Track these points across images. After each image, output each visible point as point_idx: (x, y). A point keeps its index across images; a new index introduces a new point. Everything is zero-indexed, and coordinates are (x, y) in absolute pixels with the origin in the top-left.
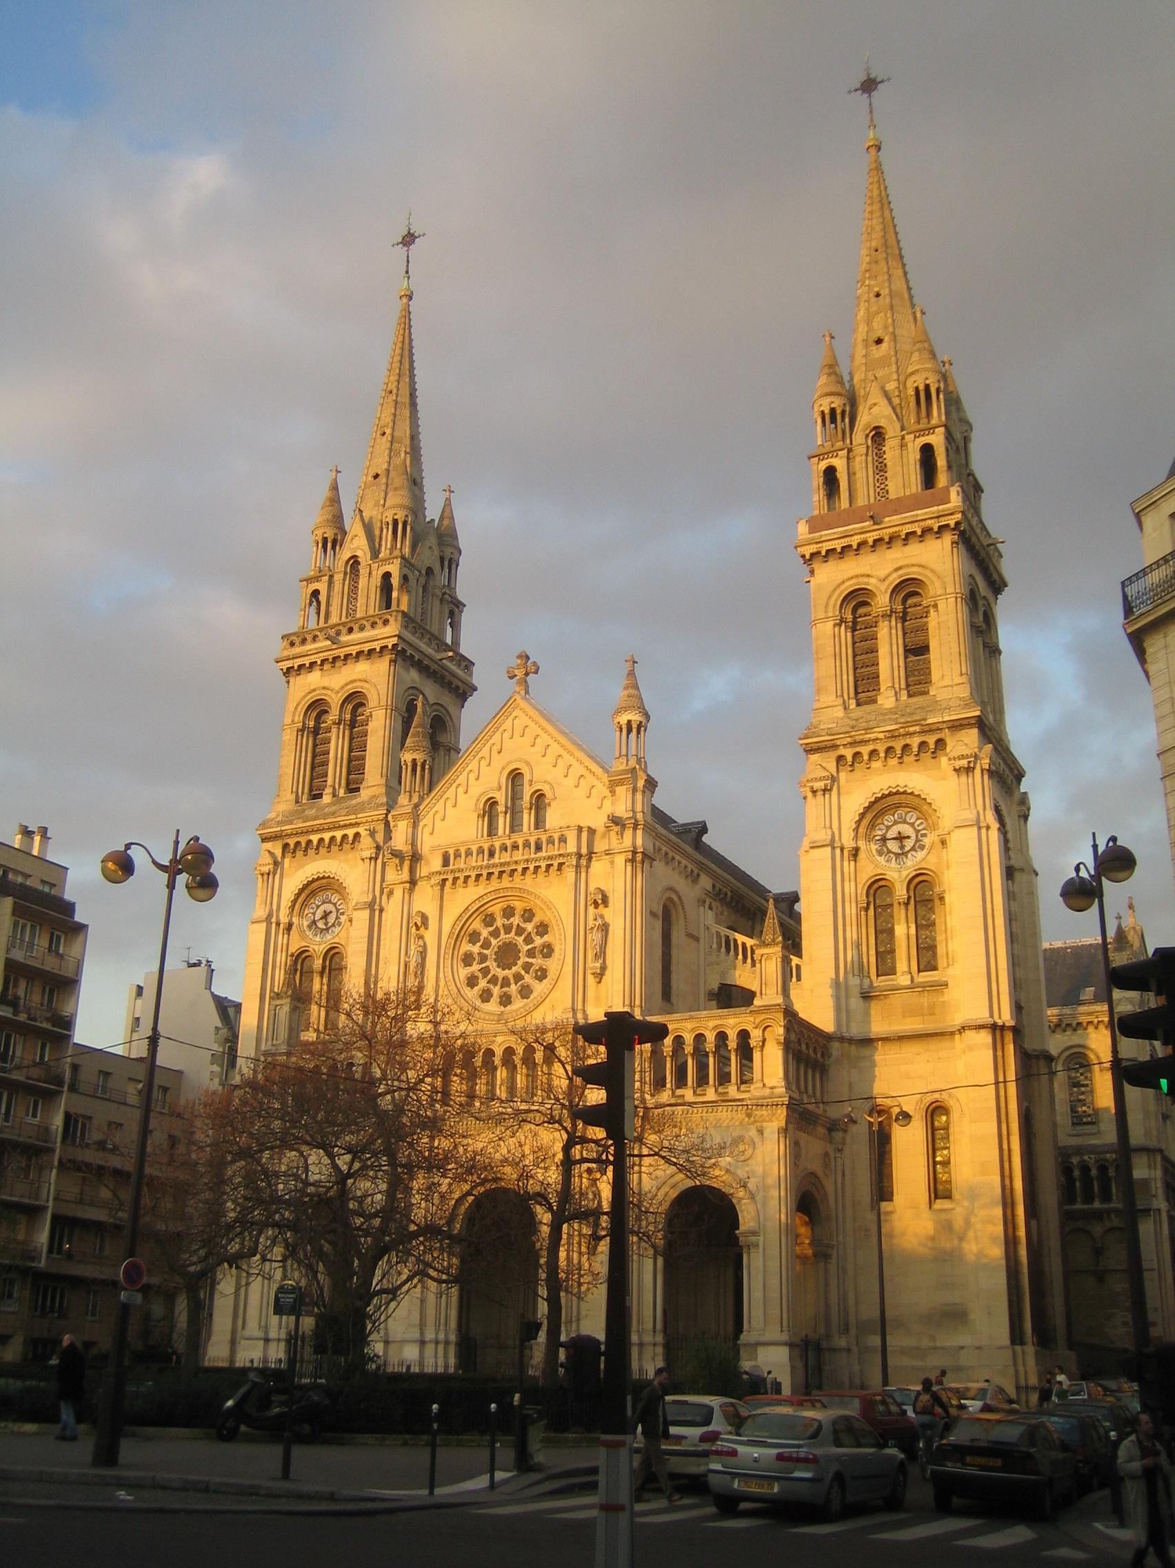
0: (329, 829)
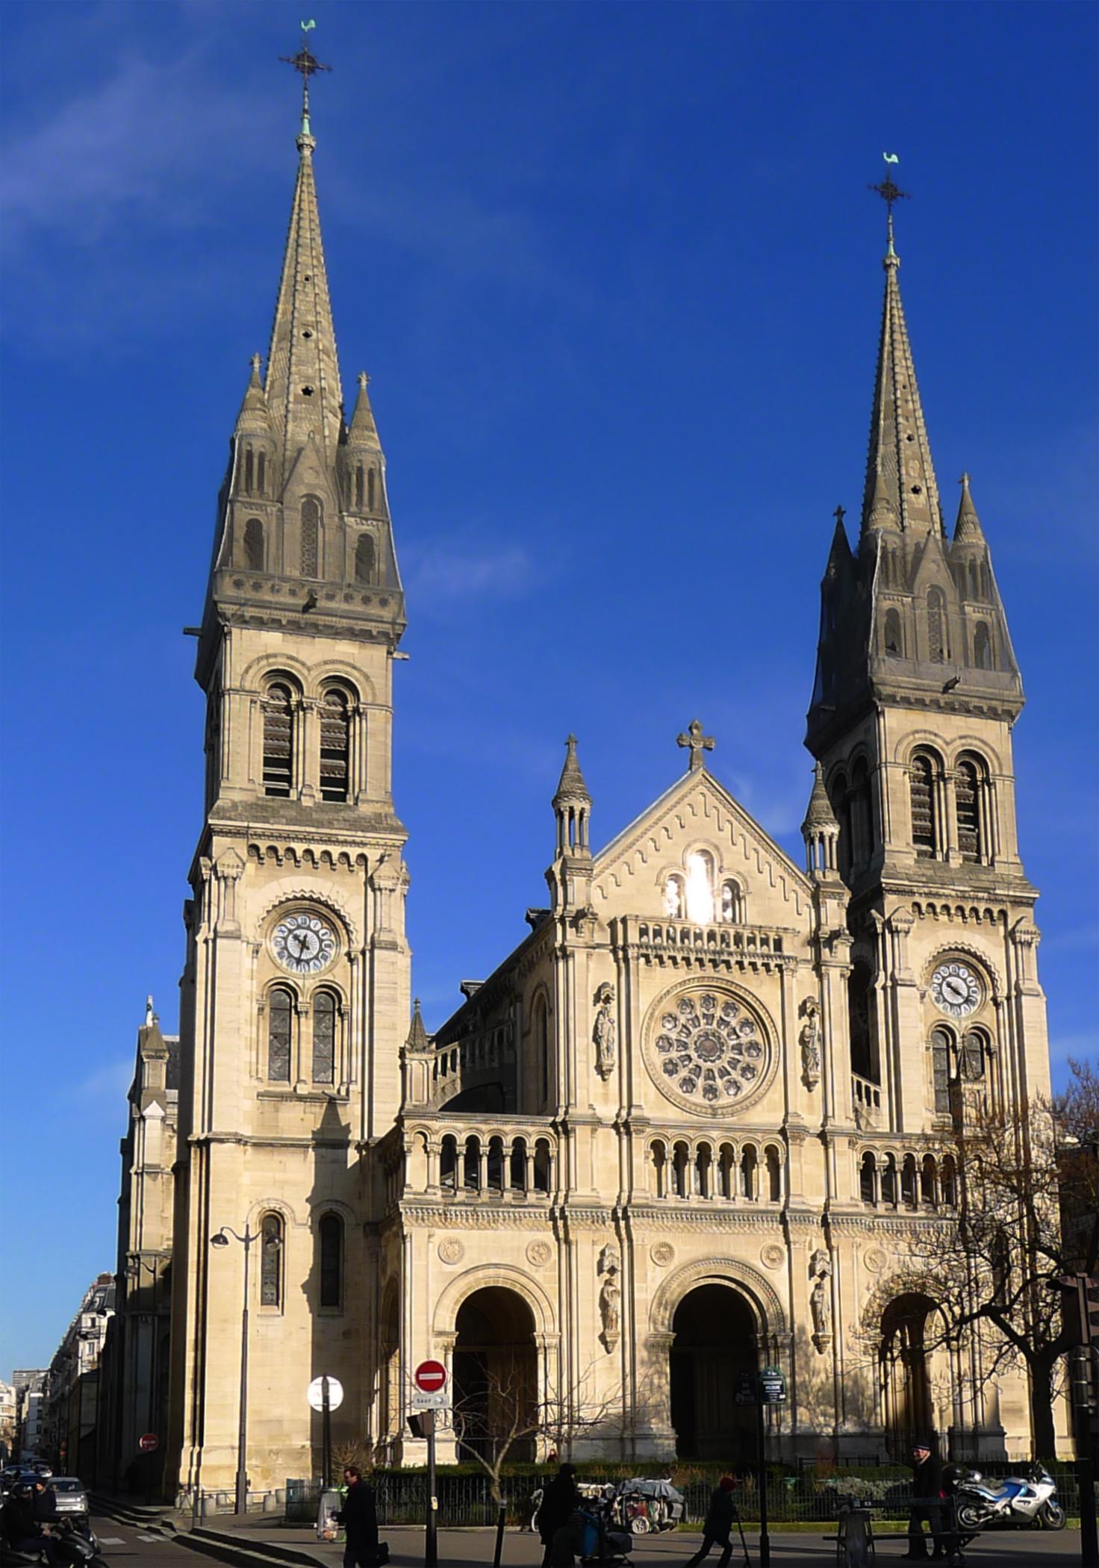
0: (321, 841)
